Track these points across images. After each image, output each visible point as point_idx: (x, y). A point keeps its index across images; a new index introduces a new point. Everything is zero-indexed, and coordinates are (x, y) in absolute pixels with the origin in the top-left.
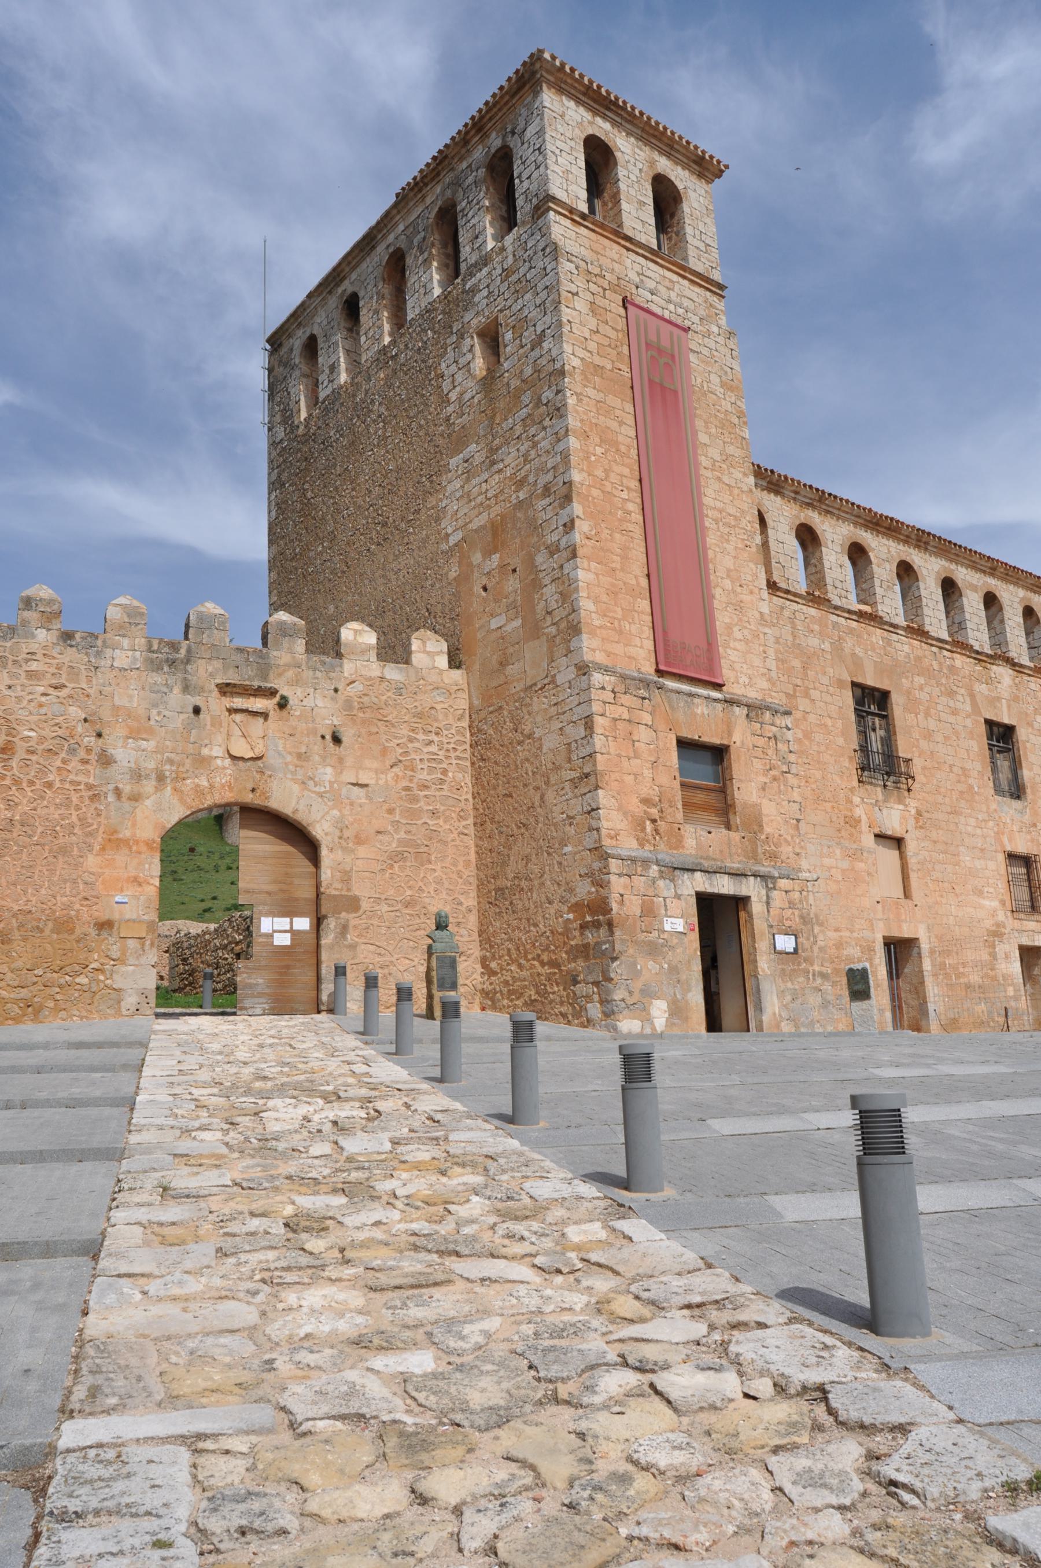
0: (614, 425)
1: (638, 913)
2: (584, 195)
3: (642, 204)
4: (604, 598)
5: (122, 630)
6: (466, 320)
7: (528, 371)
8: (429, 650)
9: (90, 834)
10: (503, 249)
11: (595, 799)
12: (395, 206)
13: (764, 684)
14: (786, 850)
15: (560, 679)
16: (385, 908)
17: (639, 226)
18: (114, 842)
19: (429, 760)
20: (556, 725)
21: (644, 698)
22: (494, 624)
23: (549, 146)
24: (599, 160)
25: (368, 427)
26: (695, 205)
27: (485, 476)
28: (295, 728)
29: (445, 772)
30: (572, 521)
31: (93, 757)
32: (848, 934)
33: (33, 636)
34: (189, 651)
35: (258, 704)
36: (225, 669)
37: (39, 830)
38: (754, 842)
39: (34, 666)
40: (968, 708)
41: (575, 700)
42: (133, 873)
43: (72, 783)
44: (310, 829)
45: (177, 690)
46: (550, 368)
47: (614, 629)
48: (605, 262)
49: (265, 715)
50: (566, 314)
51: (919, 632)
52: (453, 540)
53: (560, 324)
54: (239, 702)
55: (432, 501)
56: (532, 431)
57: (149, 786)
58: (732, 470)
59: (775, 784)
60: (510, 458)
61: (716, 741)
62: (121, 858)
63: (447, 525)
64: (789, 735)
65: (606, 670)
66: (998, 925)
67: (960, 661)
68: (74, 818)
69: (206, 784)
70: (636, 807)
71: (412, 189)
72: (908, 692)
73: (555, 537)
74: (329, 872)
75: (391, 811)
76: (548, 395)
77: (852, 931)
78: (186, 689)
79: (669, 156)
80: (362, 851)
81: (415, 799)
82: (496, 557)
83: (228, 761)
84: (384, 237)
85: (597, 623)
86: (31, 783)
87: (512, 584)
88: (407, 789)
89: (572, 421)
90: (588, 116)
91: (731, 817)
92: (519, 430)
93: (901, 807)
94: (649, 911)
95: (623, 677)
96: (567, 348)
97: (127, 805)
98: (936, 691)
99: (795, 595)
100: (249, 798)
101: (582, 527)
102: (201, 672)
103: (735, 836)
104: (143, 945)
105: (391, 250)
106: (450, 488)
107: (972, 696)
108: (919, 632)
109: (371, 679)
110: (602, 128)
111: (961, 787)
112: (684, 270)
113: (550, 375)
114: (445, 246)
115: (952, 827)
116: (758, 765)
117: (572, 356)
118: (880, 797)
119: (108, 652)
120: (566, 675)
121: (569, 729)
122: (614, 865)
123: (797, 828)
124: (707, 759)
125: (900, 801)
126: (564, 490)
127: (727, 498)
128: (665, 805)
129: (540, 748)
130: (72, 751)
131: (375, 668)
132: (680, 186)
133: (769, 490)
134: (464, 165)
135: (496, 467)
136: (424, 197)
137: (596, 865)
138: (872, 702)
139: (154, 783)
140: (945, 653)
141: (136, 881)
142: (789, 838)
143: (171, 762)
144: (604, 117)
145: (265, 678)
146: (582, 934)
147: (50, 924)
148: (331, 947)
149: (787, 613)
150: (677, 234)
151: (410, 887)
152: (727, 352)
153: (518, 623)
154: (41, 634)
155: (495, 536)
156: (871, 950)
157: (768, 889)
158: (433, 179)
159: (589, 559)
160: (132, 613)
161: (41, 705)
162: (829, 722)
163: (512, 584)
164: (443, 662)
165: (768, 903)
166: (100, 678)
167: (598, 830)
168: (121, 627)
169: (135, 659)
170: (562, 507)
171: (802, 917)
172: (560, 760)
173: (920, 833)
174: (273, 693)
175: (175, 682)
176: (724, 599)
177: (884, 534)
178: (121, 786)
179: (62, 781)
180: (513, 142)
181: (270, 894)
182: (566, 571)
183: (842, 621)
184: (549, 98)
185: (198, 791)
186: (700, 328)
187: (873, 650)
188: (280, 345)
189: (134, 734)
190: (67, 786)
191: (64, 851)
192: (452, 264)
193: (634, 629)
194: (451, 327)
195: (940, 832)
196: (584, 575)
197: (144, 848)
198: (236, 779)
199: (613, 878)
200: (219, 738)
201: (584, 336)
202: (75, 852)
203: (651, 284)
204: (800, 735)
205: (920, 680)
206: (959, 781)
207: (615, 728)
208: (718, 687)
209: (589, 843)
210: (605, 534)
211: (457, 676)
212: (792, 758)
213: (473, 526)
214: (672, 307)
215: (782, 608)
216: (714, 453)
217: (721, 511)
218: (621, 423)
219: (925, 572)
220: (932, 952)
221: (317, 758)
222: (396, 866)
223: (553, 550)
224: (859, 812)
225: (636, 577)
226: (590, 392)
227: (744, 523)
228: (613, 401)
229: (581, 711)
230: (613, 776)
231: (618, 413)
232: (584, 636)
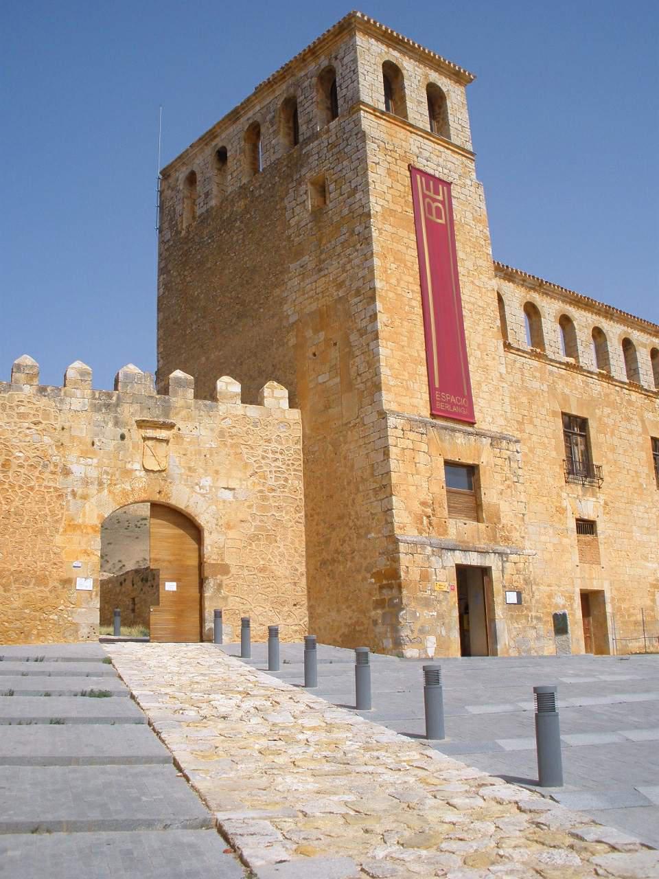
0: (403, 249)
1: (418, 579)
2: (383, 99)
3: (420, 102)
4: (397, 366)
5: (76, 384)
6: (303, 173)
7: (346, 211)
8: (275, 394)
9: (57, 521)
10: (328, 131)
11: (391, 502)
12: (254, 94)
13: (503, 422)
14: (515, 535)
15: (367, 420)
16: (246, 573)
17: (418, 117)
18: (72, 527)
19: (275, 472)
20: (363, 452)
21: (423, 434)
22: (320, 379)
23: (360, 70)
24: (392, 75)
25: (232, 237)
26: (455, 101)
27: (315, 277)
28: (186, 450)
29: (286, 480)
30: (376, 315)
31: (59, 470)
33: (21, 390)
34: (118, 398)
35: (163, 434)
36: (142, 409)
37: (26, 518)
38: (494, 530)
39: (22, 410)
40: (640, 430)
41: (377, 435)
42: (84, 547)
43: (46, 487)
44: (197, 518)
45: (110, 425)
46: (360, 211)
47: (403, 387)
48: (397, 142)
49: (167, 441)
50: (372, 176)
51: (608, 378)
52: (292, 320)
53: (367, 184)
54: (150, 433)
55: (277, 292)
56: (348, 251)
57: (93, 489)
58: (481, 276)
59: (509, 490)
60: (333, 268)
61: (471, 462)
62: (76, 537)
63: (288, 308)
64: (519, 456)
65: (398, 415)
67: (635, 396)
68: (47, 511)
69: (130, 488)
70: (417, 508)
71: (266, 85)
72: (600, 419)
73: (364, 324)
74: (209, 548)
75: (250, 507)
76: (358, 229)
77: (559, 587)
78: (116, 424)
79: (436, 71)
80: (231, 534)
81: (264, 498)
82: (322, 335)
83: (143, 473)
84: (245, 113)
85: (392, 383)
86: (21, 487)
87: (334, 354)
88: (261, 491)
89: (376, 247)
90: (384, 48)
91: (480, 513)
92: (339, 249)
93: (594, 499)
94: (425, 577)
95: (409, 420)
96: (372, 199)
97: (79, 501)
98: (619, 418)
99: (524, 352)
100: (157, 498)
101: (382, 318)
102: (126, 411)
103: (482, 526)
104: (91, 595)
105: (251, 121)
106: (290, 284)
107: (643, 421)
108: (608, 378)
109: (236, 416)
110: (395, 56)
111: (634, 485)
112: (448, 144)
113: (361, 215)
114: (288, 121)
115: (628, 513)
116: (498, 477)
117: (376, 205)
118: (580, 493)
119: (68, 400)
120: (371, 418)
121: (372, 455)
122: (402, 547)
123: (523, 520)
124: (465, 476)
125: (594, 495)
126: (370, 293)
127: (478, 295)
128: (436, 506)
129: (353, 466)
130: (45, 466)
131: (240, 408)
132: (444, 89)
133: (504, 279)
134: (303, 73)
135: (322, 273)
136: (274, 91)
137: (391, 547)
138: (576, 427)
139: (96, 487)
140: (625, 391)
141: (86, 552)
142: (517, 527)
143: (107, 473)
144: (395, 49)
145: (167, 415)
146: (380, 592)
147: (33, 581)
148: (211, 598)
149: (518, 365)
150: (443, 119)
151: (263, 559)
152: (477, 196)
153: (338, 380)
154: (27, 388)
155: (321, 319)
156: (571, 598)
157: (503, 562)
158: (280, 81)
159: (387, 340)
160: (83, 373)
161: (26, 436)
162: (546, 441)
163: (334, 354)
164: (285, 404)
165: (503, 571)
166: (62, 418)
167: (392, 523)
168: (76, 383)
169: (85, 404)
170: (369, 304)
171: (524, 580)
172: (367, 474)
173: (606, 517)
174: (172, 426)
175: (110, 418)
176: (476, 364)
177: (582, 308)
178: (75, 489)
179: (40, 486)
180: (336, 64)
181: (170, 562)
182: (371, 348)
184: (361, 40)
185: (125, 494)
186: (459, 182)
187: (576, 389)
188: (169, 176)
189: (84, 454)
190: (43, 489)
191: (41, 532)
192: (292, 133)
193: (416, 386)
194: (292, 177)
195: (620, 516)
196: (383, 352)
197: (90, 531)
198: (149, 485)
199: (401, 556)
200: (138, 457)
201: (385, 191)
202: (48, 533)
203: (426, 154)
204: (527, 451)
205: (607, 410)
206: (633, 481)
207: (403, 455)
208: (472, 424)
209: (385, 532)
210: (397, 322)
211: (295, 414)
212: (520, 472)
213: (307, 311)
214: (440, 169)
215: (515, 361)
216: (469, 264)
217: (473, 304)
218: (408, 247)
219: (611, 335)
220: (613, 599)
221: (202, 471)
222: (253, 544)
223: (362, 333)
224: (565, 503)
225: (417, 351)
226: (387, 227)
227: (489, 311)
228: (402, 232)
229: (379, 443)
230: (403, 487)
231: (405, 240)
232: (384, 392)
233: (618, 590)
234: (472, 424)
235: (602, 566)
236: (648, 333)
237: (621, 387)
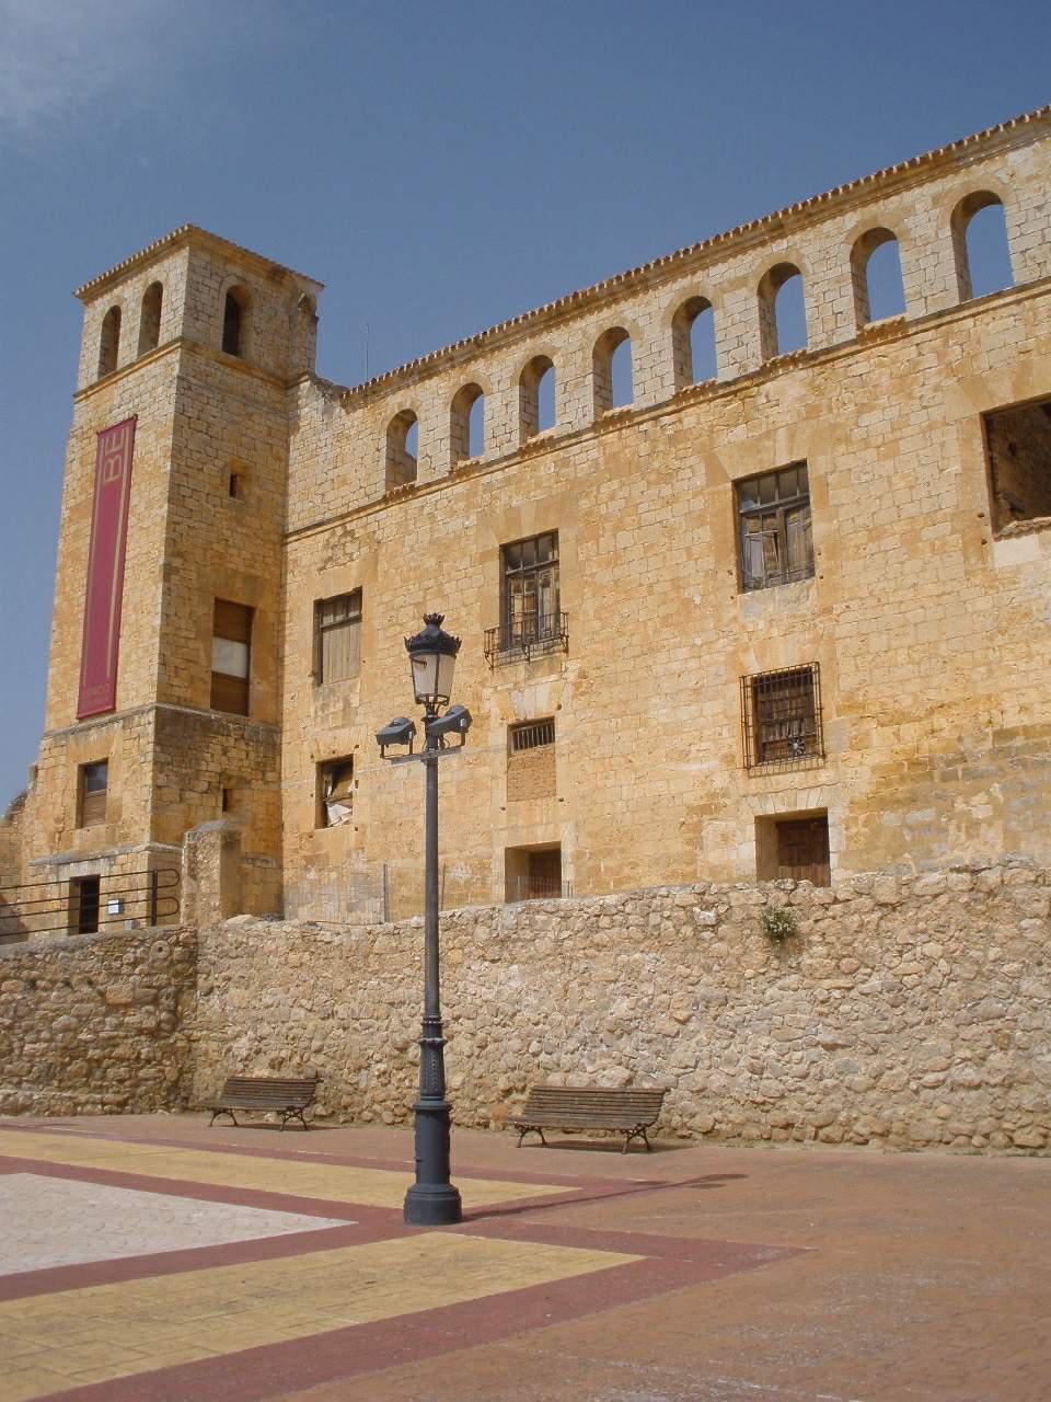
32: (456, 854)
66: (713, 795)
142: (137, 818)
144: (116, 287)
177: (573, 318)
183: (499, 475)
187: (538, 486)
220: (578, 855)
233: (593, 835)
234: (113, 710)
235: (558, 797)
236: (754, 247)
237: (655, 418)
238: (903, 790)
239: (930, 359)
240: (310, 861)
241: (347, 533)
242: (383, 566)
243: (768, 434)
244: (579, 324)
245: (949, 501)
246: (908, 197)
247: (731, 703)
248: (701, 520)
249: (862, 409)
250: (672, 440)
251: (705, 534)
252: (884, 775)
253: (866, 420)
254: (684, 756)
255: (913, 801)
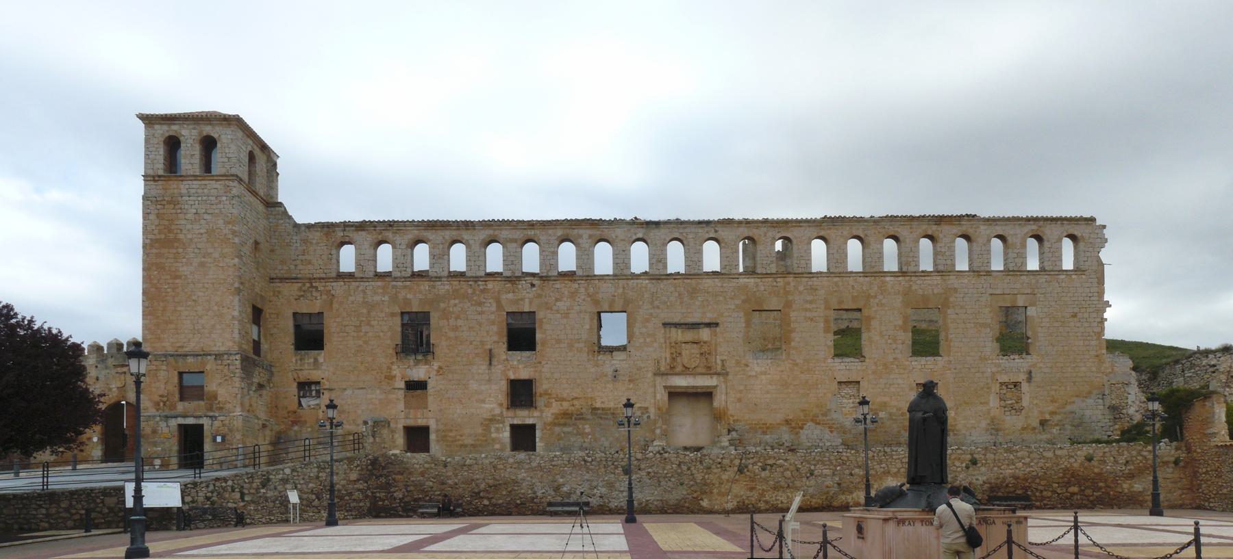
94: (154, 432)
238: (562, 421)
239: (582, 290)
240: (294, 423)
241: (312, 286)
242: (335, 306)
243: (522, 299)
244: (440, 233)
245: (584, 336)
246: (581, 232)
247: (504, 385)
248: (493, 323)
249: (557, 300)
250: (483, 291)
251: (495, 328)
252: (556, 416)
253: (558, 304)
254: (483, 401)
255: (565, 425)
